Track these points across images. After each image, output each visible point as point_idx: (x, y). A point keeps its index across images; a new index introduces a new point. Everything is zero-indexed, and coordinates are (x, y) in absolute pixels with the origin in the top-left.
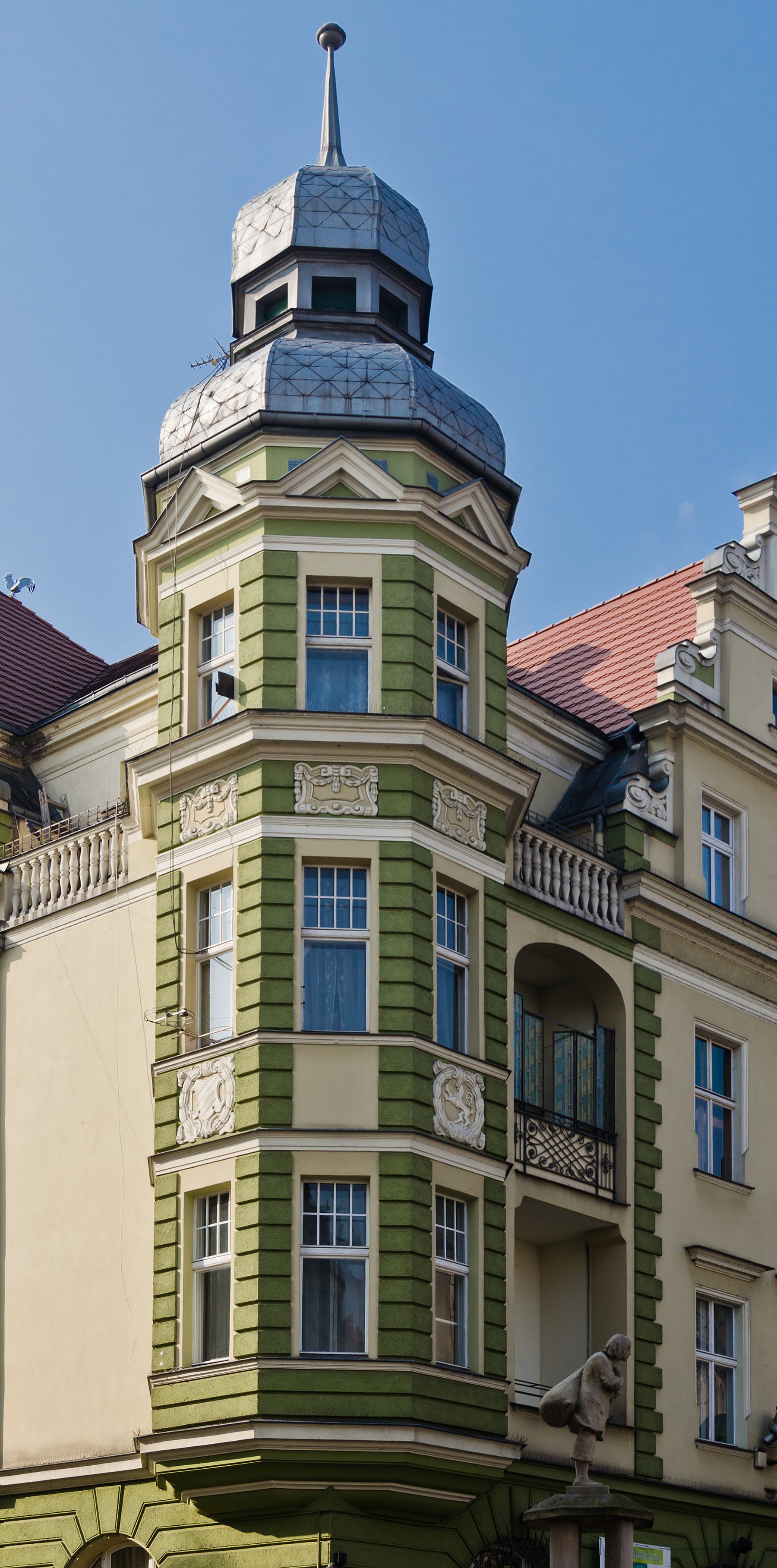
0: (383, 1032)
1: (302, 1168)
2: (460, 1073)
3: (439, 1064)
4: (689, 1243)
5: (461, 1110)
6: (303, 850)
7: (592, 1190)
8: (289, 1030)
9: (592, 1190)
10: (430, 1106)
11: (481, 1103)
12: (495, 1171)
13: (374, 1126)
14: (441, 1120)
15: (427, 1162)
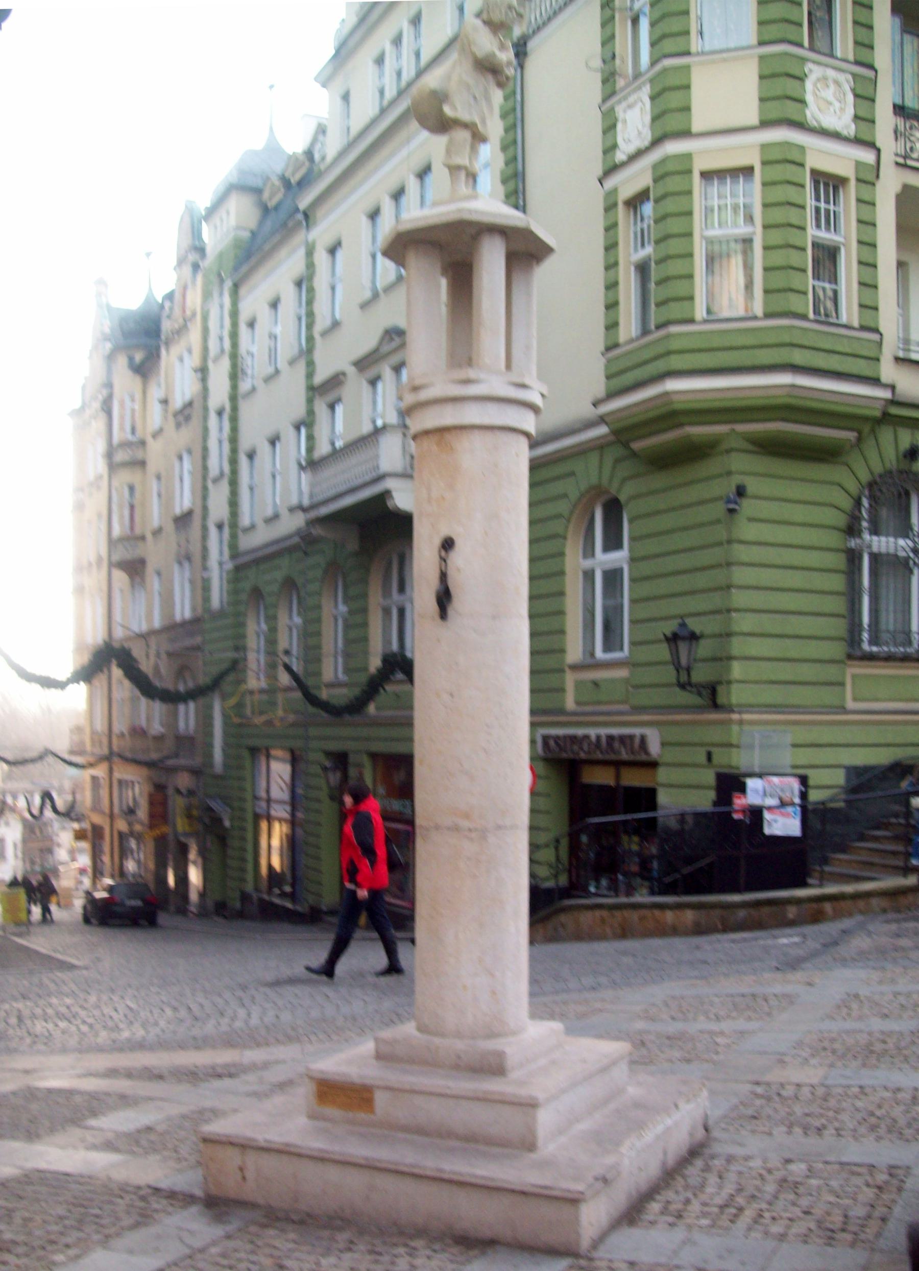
1: (699, 165)
2: (831, 73)
3: (809, 66)
5: (830, 104)
10: (802, 102)
11: (850, 98)
12: (868, 157)
13: (754, 120)
14: (814, 113)
15: (802, 149)
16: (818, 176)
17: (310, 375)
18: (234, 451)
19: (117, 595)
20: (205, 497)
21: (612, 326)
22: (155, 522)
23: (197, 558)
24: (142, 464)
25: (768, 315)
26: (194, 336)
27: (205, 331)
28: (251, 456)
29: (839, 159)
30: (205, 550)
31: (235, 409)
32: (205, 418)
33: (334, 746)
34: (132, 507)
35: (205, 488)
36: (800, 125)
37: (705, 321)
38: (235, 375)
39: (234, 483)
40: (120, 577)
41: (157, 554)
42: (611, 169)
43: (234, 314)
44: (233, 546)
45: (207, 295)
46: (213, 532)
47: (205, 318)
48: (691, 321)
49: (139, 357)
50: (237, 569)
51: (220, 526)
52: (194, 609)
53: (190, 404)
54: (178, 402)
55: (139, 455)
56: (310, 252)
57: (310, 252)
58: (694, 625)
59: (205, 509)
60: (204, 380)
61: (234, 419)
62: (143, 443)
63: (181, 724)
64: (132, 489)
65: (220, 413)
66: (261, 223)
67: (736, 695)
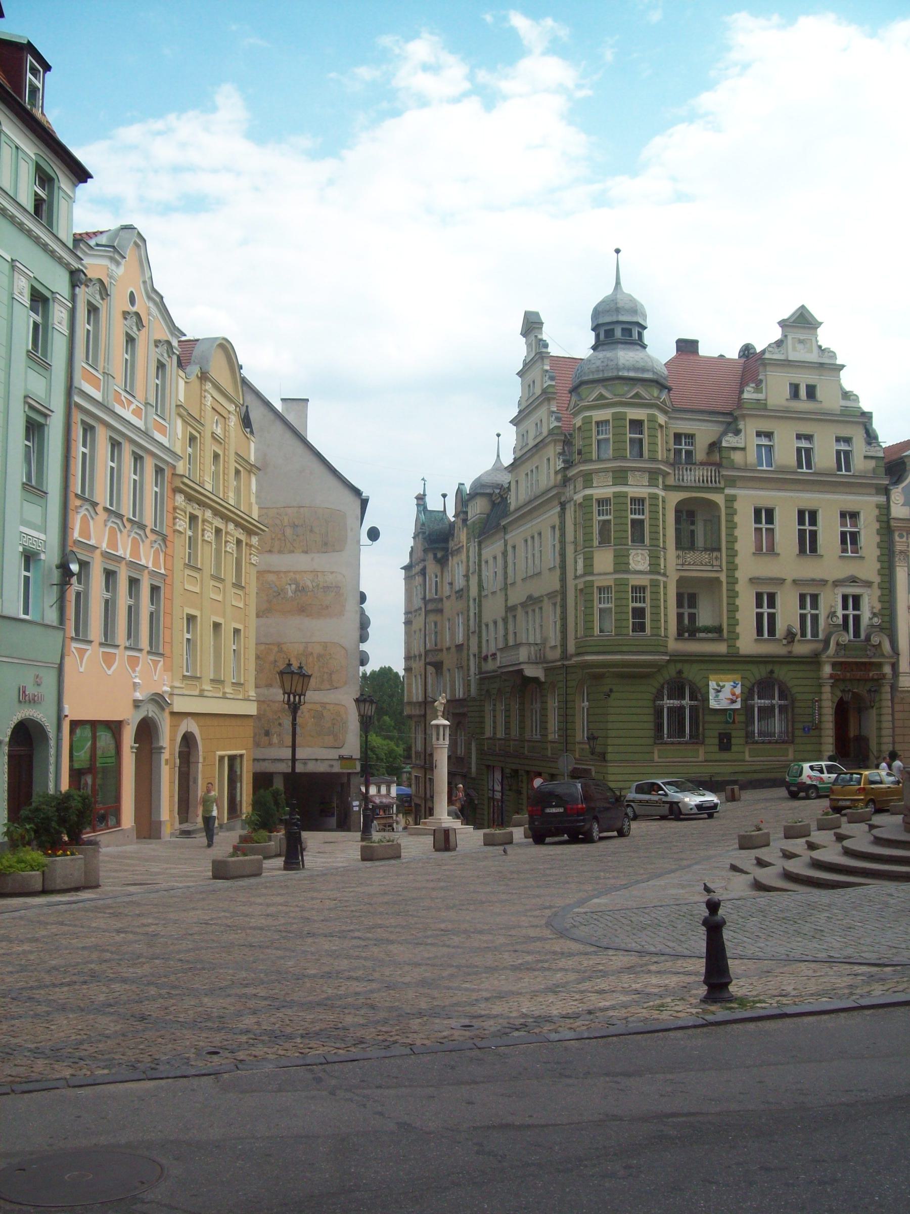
0: (615, 545)
2: (639, 551)
4: (750, 576)
6: (595, 497)
7: (710, 568)
8: (592, 547)
9: (710, 568)
10: (628, 564)
13: (612, 571)
14: (633, 566)
16: (635, 589)
17: (506, 600)
18: (480, 621)
19: (429, 681)
20: (468, 640)
22: (448, 645)
23: (465, 668)
24: (441, 611)
25: (616, 635)
26: (464, 556)
27: (468, 557)
29: (643, 580)
30: (468, 665)
31: (480, 601)
33: (514, 767)
34: (436, 633)
35: (468, 635)
36: (627, 571)
37: (599, 636)
39: (480, 637)
40: (431, 669)
41: (449, 661)
43: (480, 555)
44: (480, 668)
46: (472, 657)
47: (468, 551)
48: (593, 636)
49: (439, 555)
50: (481, 679)
51: (475, 655)
52: (464, 694)
53: (462, 590)
55: (440, 606)
56: (506, 545)
57: (506, 545)
58: (596, 735)
59: (468, 646)
61: (480, 606)
62: (441, 600)
63: (459, 752)
64: (436, 624)
65: (475, 600)
66: (492, 510)
67: (609, 757)
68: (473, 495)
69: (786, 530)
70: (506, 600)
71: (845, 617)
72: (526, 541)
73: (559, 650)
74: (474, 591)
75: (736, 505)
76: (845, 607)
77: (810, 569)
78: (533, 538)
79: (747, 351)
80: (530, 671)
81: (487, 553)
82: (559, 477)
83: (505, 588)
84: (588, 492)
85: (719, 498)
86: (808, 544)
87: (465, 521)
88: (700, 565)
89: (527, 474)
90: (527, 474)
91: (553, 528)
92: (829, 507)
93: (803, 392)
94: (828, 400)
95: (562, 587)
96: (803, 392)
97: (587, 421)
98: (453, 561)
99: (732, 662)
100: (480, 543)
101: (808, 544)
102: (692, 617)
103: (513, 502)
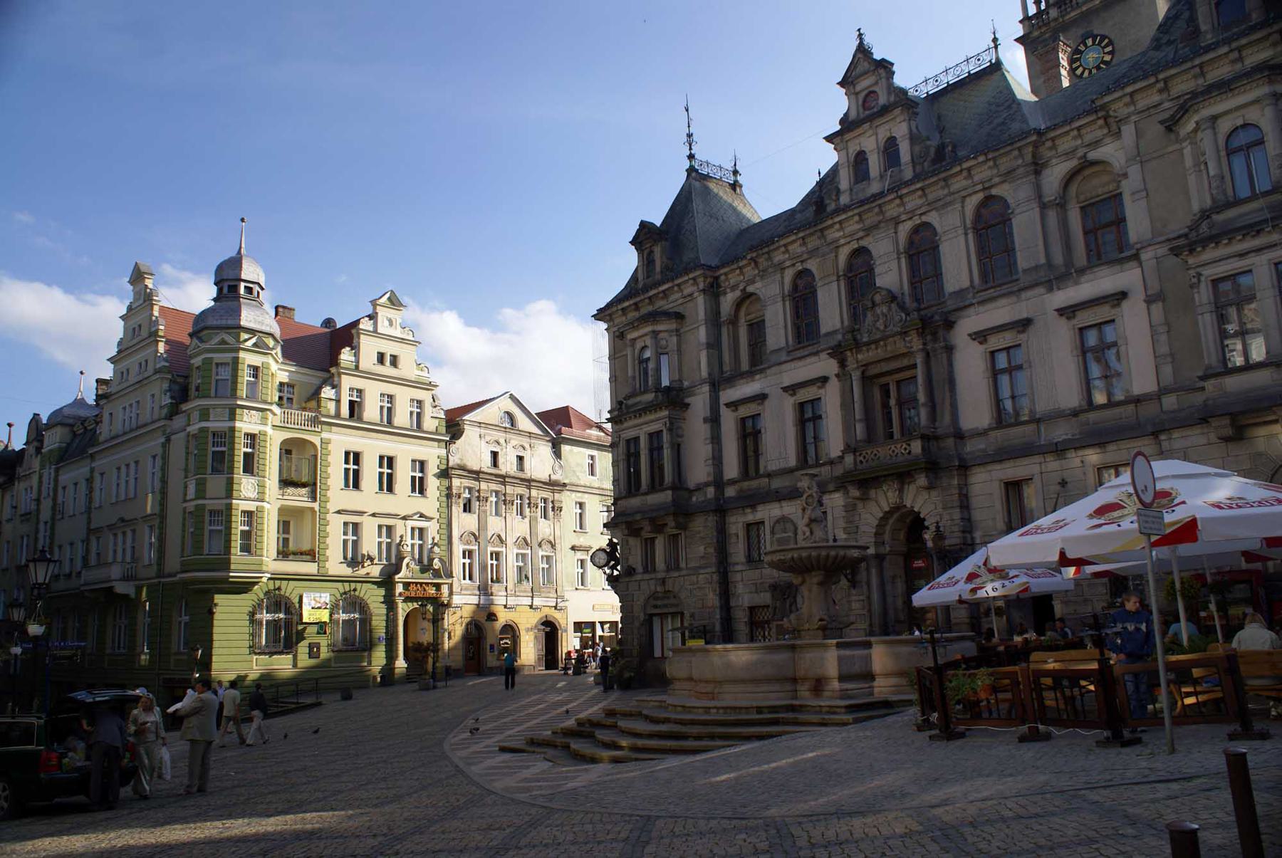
17: (89, 523)
21: (183, 550)
26: (35, 480)
27: (40, 482)
28: (60, 547)
29: (251, 506)
32: (38, 523)
38: (54, 508)
42: (185, 501)
43: (56, 481)
45: (42, 467)
54: (22, 510)
56: (92, 470)
60: (38, 505)
61: (53, 528)
65: (46, 523)
66: (72, 440)
68: (49, 426)
69: (370, 471)
70: (89, 523)
71: (413, 545)
72: (119, 469)
73: (155, 567)
74: (45, 514)
75: (330, 447)
76: (413, 538)
77: (386, 503)
78: (128, 466)
79: (328, 322)
80: (121, 588)
81: (66, 477)
82: (165, 411)
83: (89, 510)
84: (204, 424)
85: (316, 440)
86: (387, 484)
87: (38, 450)
88: (298, 497)
89: (124, 408)
90: (124, 408)
91: (154, 457)
92: (405, 452)
93: (388, 360)
94: (407, 369)
95: (162, 510)
96: (388, 360)
97: (208, 362)
98: (20, 487)
99: (322, 579)
100: (57, 471)
101: (387, 484)
102: (286, 541)
103: (104, 431)
